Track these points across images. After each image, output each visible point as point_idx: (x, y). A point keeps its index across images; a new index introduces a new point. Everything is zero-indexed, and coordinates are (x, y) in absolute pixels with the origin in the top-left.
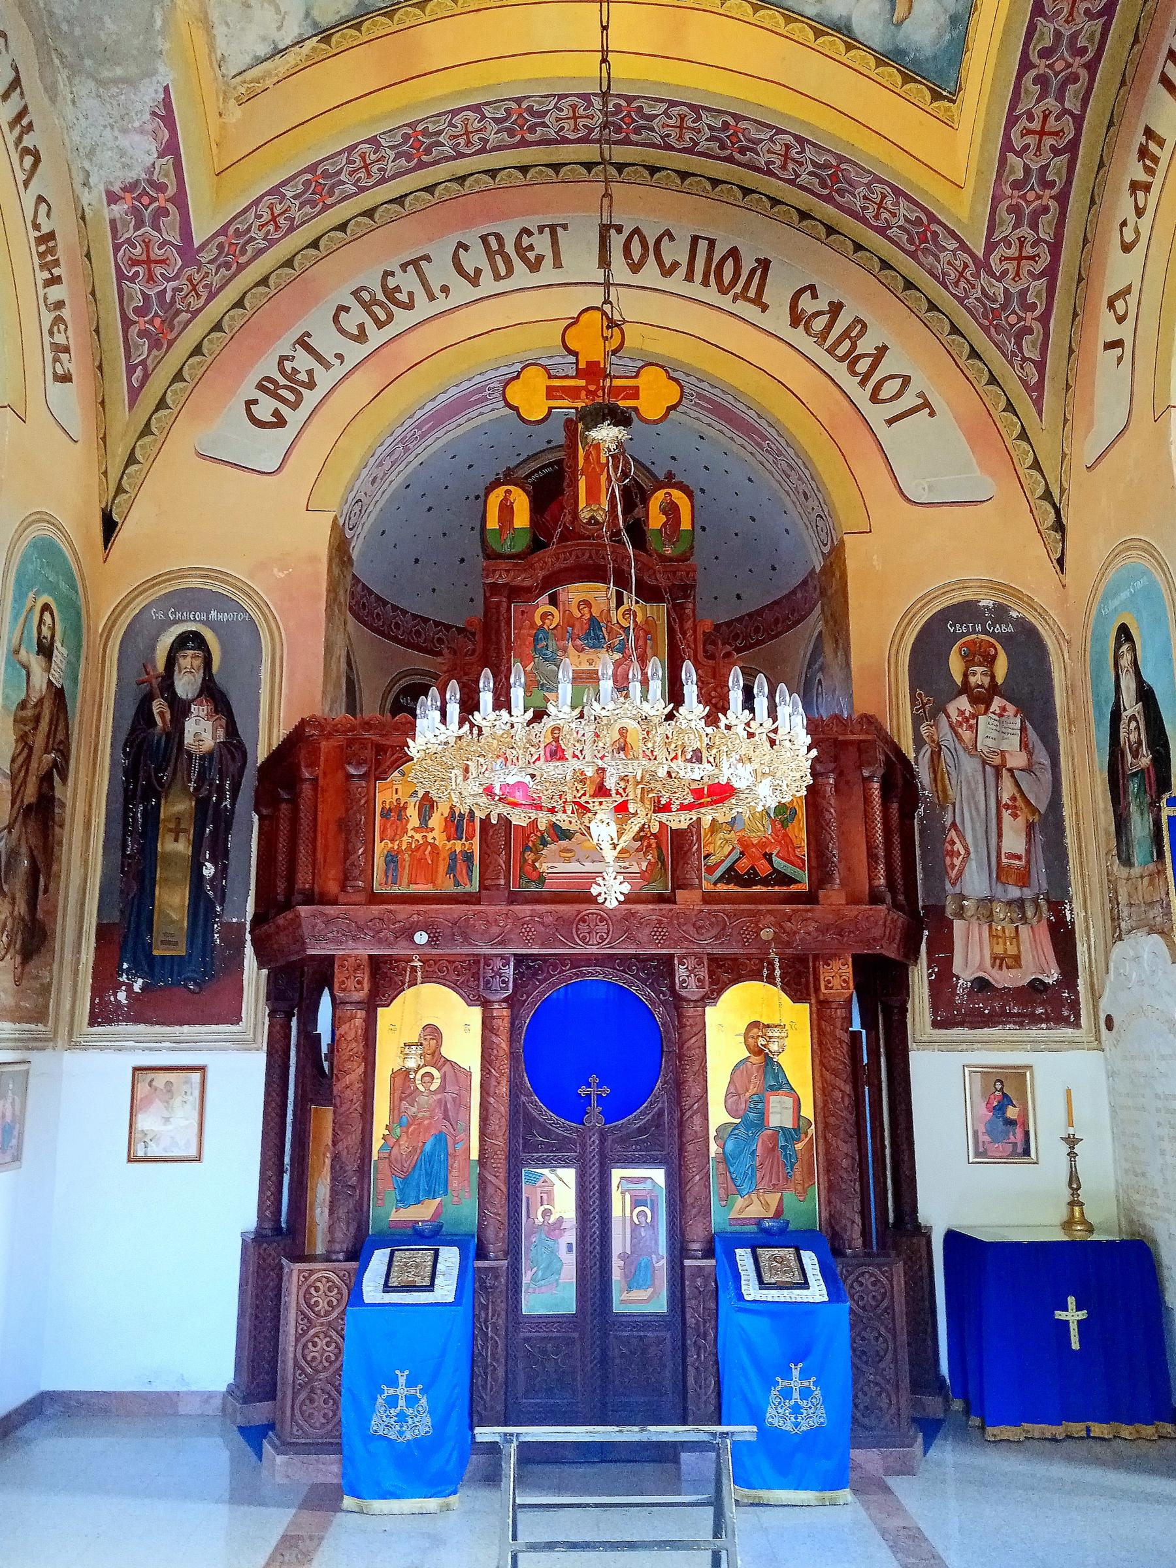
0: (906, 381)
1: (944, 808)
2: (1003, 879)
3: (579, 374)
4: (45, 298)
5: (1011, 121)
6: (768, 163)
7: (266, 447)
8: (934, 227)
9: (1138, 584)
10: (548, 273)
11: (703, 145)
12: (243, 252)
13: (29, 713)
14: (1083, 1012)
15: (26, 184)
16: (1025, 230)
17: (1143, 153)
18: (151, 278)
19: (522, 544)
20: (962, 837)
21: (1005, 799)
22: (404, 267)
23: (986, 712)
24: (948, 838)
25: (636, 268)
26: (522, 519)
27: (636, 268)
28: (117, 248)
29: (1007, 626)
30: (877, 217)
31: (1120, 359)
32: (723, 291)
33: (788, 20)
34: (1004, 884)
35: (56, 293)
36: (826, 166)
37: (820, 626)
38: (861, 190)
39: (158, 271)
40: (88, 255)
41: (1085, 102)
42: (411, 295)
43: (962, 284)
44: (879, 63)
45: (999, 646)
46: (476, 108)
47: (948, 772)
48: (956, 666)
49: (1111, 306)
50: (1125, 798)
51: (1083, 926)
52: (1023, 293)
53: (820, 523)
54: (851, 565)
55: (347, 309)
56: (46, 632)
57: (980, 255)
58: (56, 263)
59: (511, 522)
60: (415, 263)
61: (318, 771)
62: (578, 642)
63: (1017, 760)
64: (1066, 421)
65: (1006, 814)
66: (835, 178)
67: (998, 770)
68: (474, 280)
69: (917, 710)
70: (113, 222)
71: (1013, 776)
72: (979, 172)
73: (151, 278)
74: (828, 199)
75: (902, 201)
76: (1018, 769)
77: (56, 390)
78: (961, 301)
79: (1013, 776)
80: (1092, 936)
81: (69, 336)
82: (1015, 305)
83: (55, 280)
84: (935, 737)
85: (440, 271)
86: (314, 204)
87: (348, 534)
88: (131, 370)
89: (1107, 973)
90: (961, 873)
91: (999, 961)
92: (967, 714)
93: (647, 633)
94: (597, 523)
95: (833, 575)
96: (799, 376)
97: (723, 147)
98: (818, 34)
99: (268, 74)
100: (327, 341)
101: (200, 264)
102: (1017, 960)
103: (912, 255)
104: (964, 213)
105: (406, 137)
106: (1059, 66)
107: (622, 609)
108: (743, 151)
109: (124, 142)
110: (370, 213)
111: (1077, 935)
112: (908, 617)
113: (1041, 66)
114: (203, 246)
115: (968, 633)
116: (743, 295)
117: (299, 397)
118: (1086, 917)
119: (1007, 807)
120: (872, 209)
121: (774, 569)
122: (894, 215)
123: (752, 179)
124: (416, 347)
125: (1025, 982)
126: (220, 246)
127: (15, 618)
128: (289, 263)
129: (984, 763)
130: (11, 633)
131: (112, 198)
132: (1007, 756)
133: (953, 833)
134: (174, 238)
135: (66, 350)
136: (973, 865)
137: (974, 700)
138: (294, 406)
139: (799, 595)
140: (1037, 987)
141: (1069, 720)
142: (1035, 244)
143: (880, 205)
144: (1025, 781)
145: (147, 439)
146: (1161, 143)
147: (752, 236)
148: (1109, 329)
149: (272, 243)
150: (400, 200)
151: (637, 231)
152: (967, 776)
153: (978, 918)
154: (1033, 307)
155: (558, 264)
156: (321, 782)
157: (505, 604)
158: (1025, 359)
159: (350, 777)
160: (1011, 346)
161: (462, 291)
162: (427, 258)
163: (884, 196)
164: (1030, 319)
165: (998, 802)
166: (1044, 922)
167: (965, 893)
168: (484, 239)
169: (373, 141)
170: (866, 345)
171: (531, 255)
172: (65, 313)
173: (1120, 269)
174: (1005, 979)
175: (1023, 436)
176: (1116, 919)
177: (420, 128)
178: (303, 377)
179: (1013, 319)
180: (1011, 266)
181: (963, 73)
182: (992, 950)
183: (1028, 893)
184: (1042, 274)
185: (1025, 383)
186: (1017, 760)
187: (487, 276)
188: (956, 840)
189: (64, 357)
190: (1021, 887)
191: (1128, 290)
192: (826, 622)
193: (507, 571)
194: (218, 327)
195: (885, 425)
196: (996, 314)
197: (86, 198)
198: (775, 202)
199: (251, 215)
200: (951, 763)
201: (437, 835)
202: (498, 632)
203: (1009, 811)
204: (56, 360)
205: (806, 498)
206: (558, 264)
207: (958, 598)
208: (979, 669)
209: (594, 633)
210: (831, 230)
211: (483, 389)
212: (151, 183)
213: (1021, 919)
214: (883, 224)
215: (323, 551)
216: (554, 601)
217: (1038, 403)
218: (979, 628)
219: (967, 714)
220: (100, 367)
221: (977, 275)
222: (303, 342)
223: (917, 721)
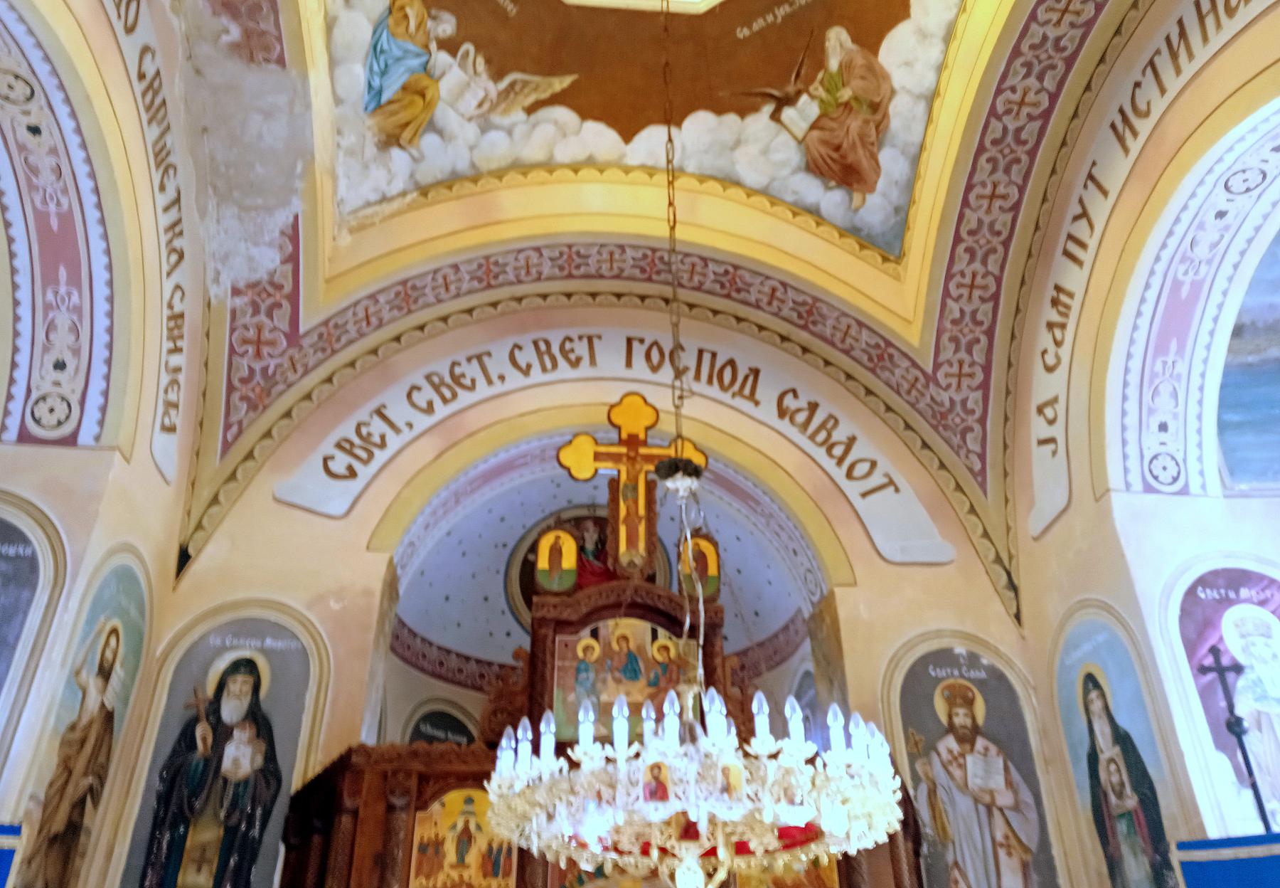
0: (874, 464)
3: (621, 442)
4: (167, 363)
5: (949, 277)
6: (757, 301)
7: (338, 496)
8: (891, 350)
9: (1101, 638)
10: (585, 370)
11: (708, 285)
12: (338, 339)
13: (77, 735)
15: (169, 274)
16: (963, 355)
17: (1055, 302)
18: (258, 354)
19: (569, 582)
22: (469, 360)
25: (655, 369)
26: (569, 560)
27: (655, 369)
28: (232, 331)
30: (843, 341)
31: (1054, 453)
32: (723, 388)
33: (773, 204)
35: (176, 360)
36: (804, 304)
37: (810, 666)
38: (830, 323)
39: (265, 350)
40: (208, 335)
41: (1002, 268)
42: (473, 381)
43: (914, 393)
44: (841, 236)
46: (538, 250)
49: (1040, 410)
52: (964, 402)
53: (809, 576)
54: (843, 613)
55: (419, 389)
56: (109, 655)
57: (929, 369)
58: (181, 337)
59: (560, 562)
60: (479, 358)
61: (360, 802)
62: (617, 674)
64: (1007, 501)
66: (810, 313)
68: (526, 371)
70: (234, 312)
72: (926, 312)
73: (258, 354)
74: (805, 327)
75: (864, 332)
77: (161, 439)
78: (913, 405)
81: (180, 396)
82: (958, 408)
83: (177, 350)
85: (498, 363)
86: (400, 308)
87: (399, 571)
88: (227, 427)
93: (679, 667)
94: (635, 565)
95: (823, 620)
96: (789, 458)
97: (723, 286)
98: (795, 214)
99: (377, 214)
100: (399, 411)
101: (301, 348)
103: (873, 371)
104: (915, 340)
105: (480, 266)
106: (982, 242)
107: (657, 644)
108: (738, 291)
109: (254, 251)
110: (445, 319)
112: (894, 661)
113: (969, 241)
114: (307, 333)
115: (948, 677)
116: (740, 393)
117: (371, 455)
120: (839, 335)
121: (757, 614)
122: (857, 340)
123: (743, 311)
124: (474, 419)
126: (321, 336)
127: (84, 639)
128: (374, 352)
130: (77, 654)
131: (236, 292)
134: (285, 326)
135: (176, 406)
138: (365, 463)
139: (781, 638)
142: (972, 364)
143: (846, 333)
145: (232, 485)
146: (1071, 295)
147: (747, 352)
148: (1044, 431)
149: (362, 335)
150: (470, 311)
151: (656, 343)
154: (973, 412)
155: (593, 361)
156: (361, 813)
157: (550, 638)
158: (969, 451)
159: (391, 808)
160: (956, 440)
161: (515, 379)
162: (489, 354)
163: (849, 327)
164: (971, 421)
168: (536, 343)
169: (456, 267)
170: (840, 435)
171: (572, 357)
172: (181, 378)
173: (1044, 386)
175: (972, 510)
177: (492, 260)
178: (377, 439)
179: (958, 420)
180: (954, 381)
181: (906, 246)
184: (977, 388)
185: (971, 470)
187: (536, 368)
189: (173, 412)
191: (1055, 400)
192: (817, 663)
193: (555, 606)
194: (308, 397)
195: (859, 498)
196: (944, 416)
197: (214, 291)
198: (761, 328)
199: (350, 313)
201: (472, 873)
202: (544, 663)
204: (166, 413)
205: (795, 552)
206: (593, 361)
207: (934, 645)
209: (630, 666)
210: (805, 350)
211: (525, 456)
212: (272, 283)
214: (846, 346)
215: (377, 586)
216: (595, 634)
217: (983, 486)
220: (201, 424)
221: (927, 386)
222: (380, 413)
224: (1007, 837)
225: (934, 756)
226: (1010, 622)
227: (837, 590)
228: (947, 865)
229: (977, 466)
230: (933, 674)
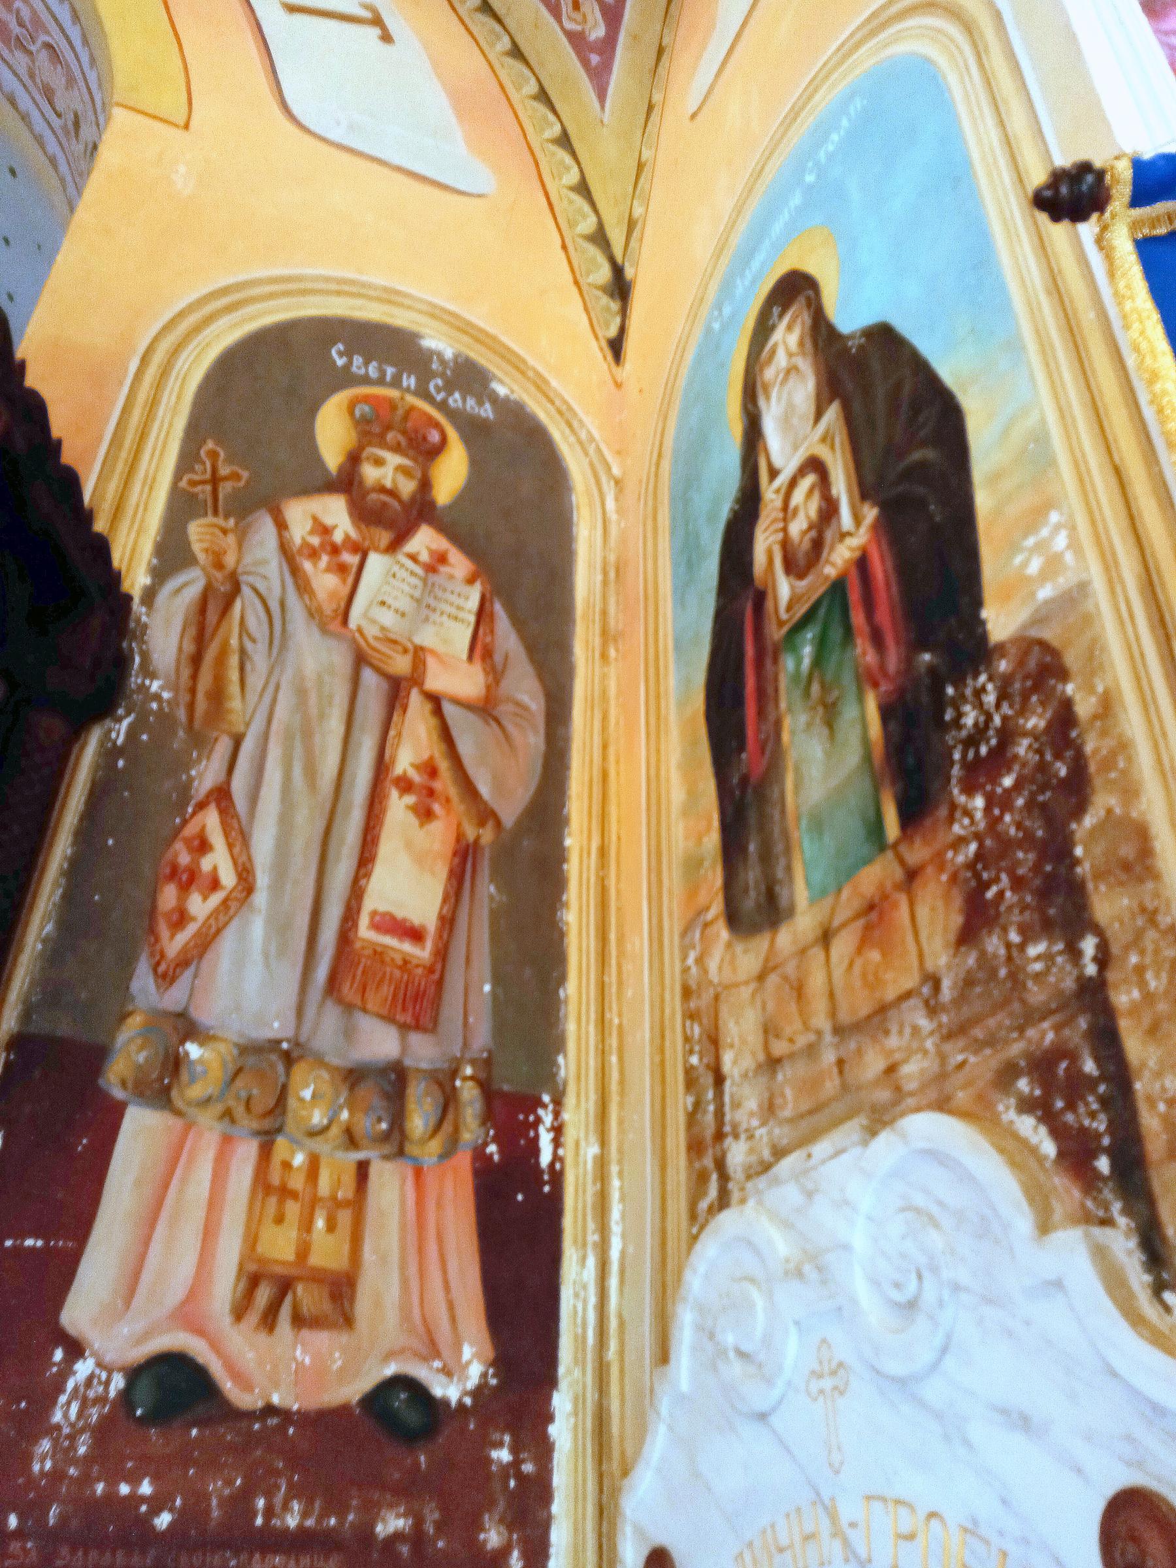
1: (200, 741)
2: (348, 990)
14: (560, 1536)
20: (239, 837)
21: (405, 761)
23: (394, 546)
24: (190, 830)
29: (480, 403)
34: (349, 1008)
45: (452, 434)
47: (243, 652)
48: (332, 433)
50: (761, 713)
51: (591, 1190)
63: (457, 679)
65: (398, 807)
67: (397, 692)
69: (193, 483)
71: (438, 711)
76: (457, 702)
79: (438, 711)
80: (616, 1229)
84: (230, 560)
89: (663, 1356)
90: (205, 942)
91: (271, 1293)
92: (338, 537)
102: (340, 1298)
111: (568, 1222)
112: (231, 298)
115: (381, 381)
118: (602, 1163)
119: (405, 785)
125: (353, 1391)
129: (360, 659)
132: (431, 661)
133: (211, 819)
136: (255, 927)
137: (363, 513)
140: (399, 1412)
141: (604, 632)
144: (470, 738)
152: (300, 677)
153: (228, 1115)
165: (382, 766)
166: (463, 1161)
167: (206, 1014)
174: (277, 1371)
176: (706, 1144)
182: (251, 1240)
183: (424, 1052)
185: (577, 40)
186: (457, 679)
188: (217, 839)
190: (404, 1028)
200: (256, 622)
203: (410, 799)
208: (393, 460)
213: (386, 1137)
217: (600, 77)
218: (410, 381)
219: (338, 537)
223: (182, 507)
224: (431, 771)
225: (265, 530)
226: (597, 354)
227: (118, 113)
228: (185, 791)
229: (598, 32)
230: (340, 362)
